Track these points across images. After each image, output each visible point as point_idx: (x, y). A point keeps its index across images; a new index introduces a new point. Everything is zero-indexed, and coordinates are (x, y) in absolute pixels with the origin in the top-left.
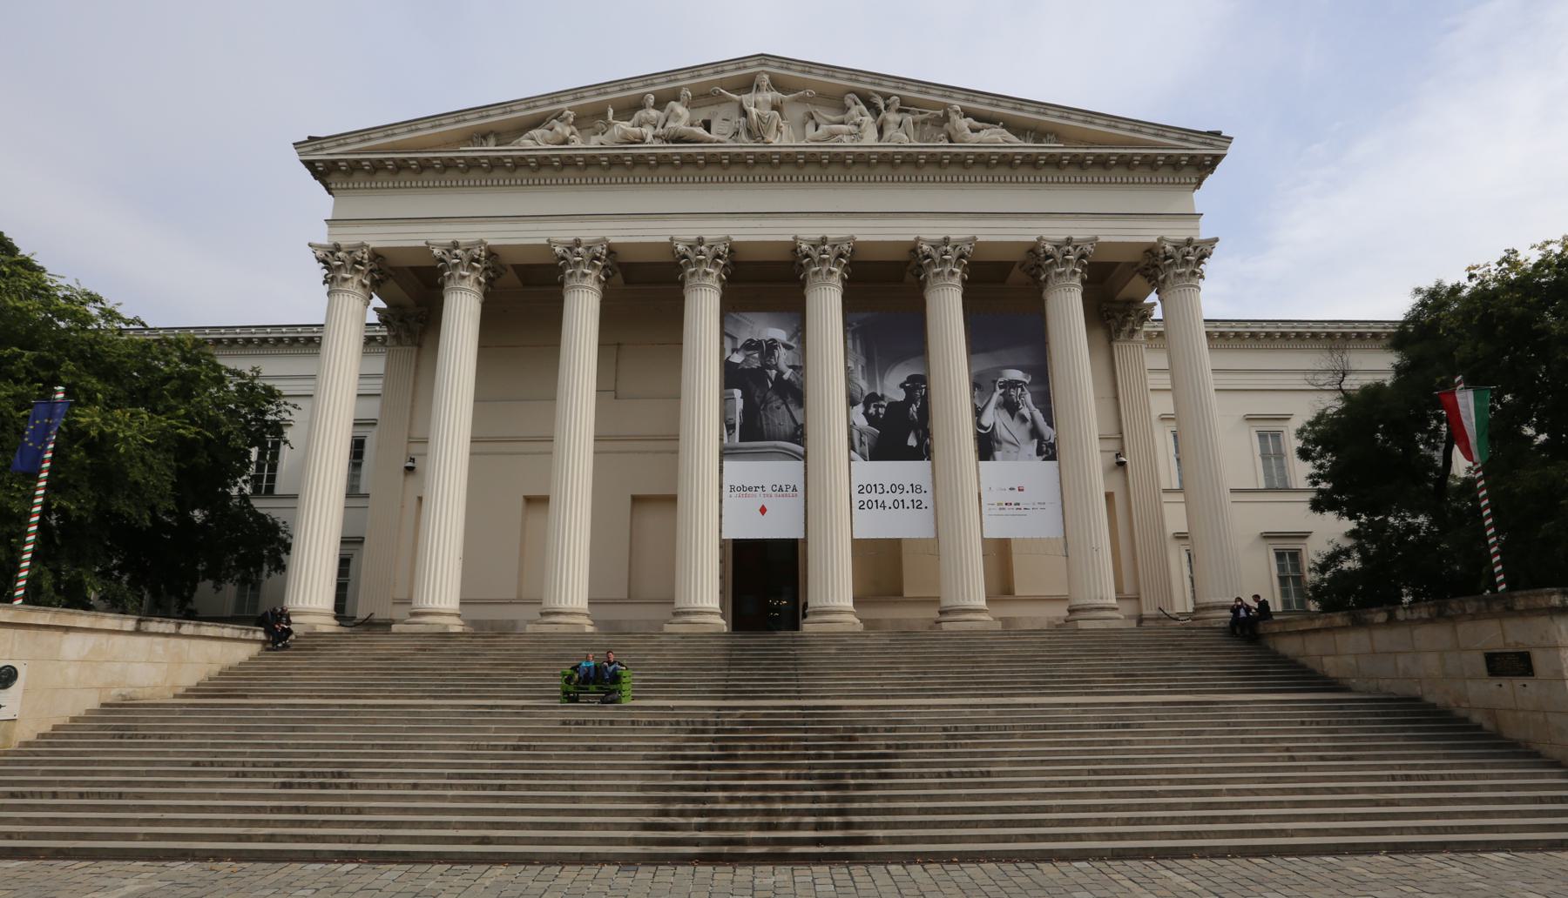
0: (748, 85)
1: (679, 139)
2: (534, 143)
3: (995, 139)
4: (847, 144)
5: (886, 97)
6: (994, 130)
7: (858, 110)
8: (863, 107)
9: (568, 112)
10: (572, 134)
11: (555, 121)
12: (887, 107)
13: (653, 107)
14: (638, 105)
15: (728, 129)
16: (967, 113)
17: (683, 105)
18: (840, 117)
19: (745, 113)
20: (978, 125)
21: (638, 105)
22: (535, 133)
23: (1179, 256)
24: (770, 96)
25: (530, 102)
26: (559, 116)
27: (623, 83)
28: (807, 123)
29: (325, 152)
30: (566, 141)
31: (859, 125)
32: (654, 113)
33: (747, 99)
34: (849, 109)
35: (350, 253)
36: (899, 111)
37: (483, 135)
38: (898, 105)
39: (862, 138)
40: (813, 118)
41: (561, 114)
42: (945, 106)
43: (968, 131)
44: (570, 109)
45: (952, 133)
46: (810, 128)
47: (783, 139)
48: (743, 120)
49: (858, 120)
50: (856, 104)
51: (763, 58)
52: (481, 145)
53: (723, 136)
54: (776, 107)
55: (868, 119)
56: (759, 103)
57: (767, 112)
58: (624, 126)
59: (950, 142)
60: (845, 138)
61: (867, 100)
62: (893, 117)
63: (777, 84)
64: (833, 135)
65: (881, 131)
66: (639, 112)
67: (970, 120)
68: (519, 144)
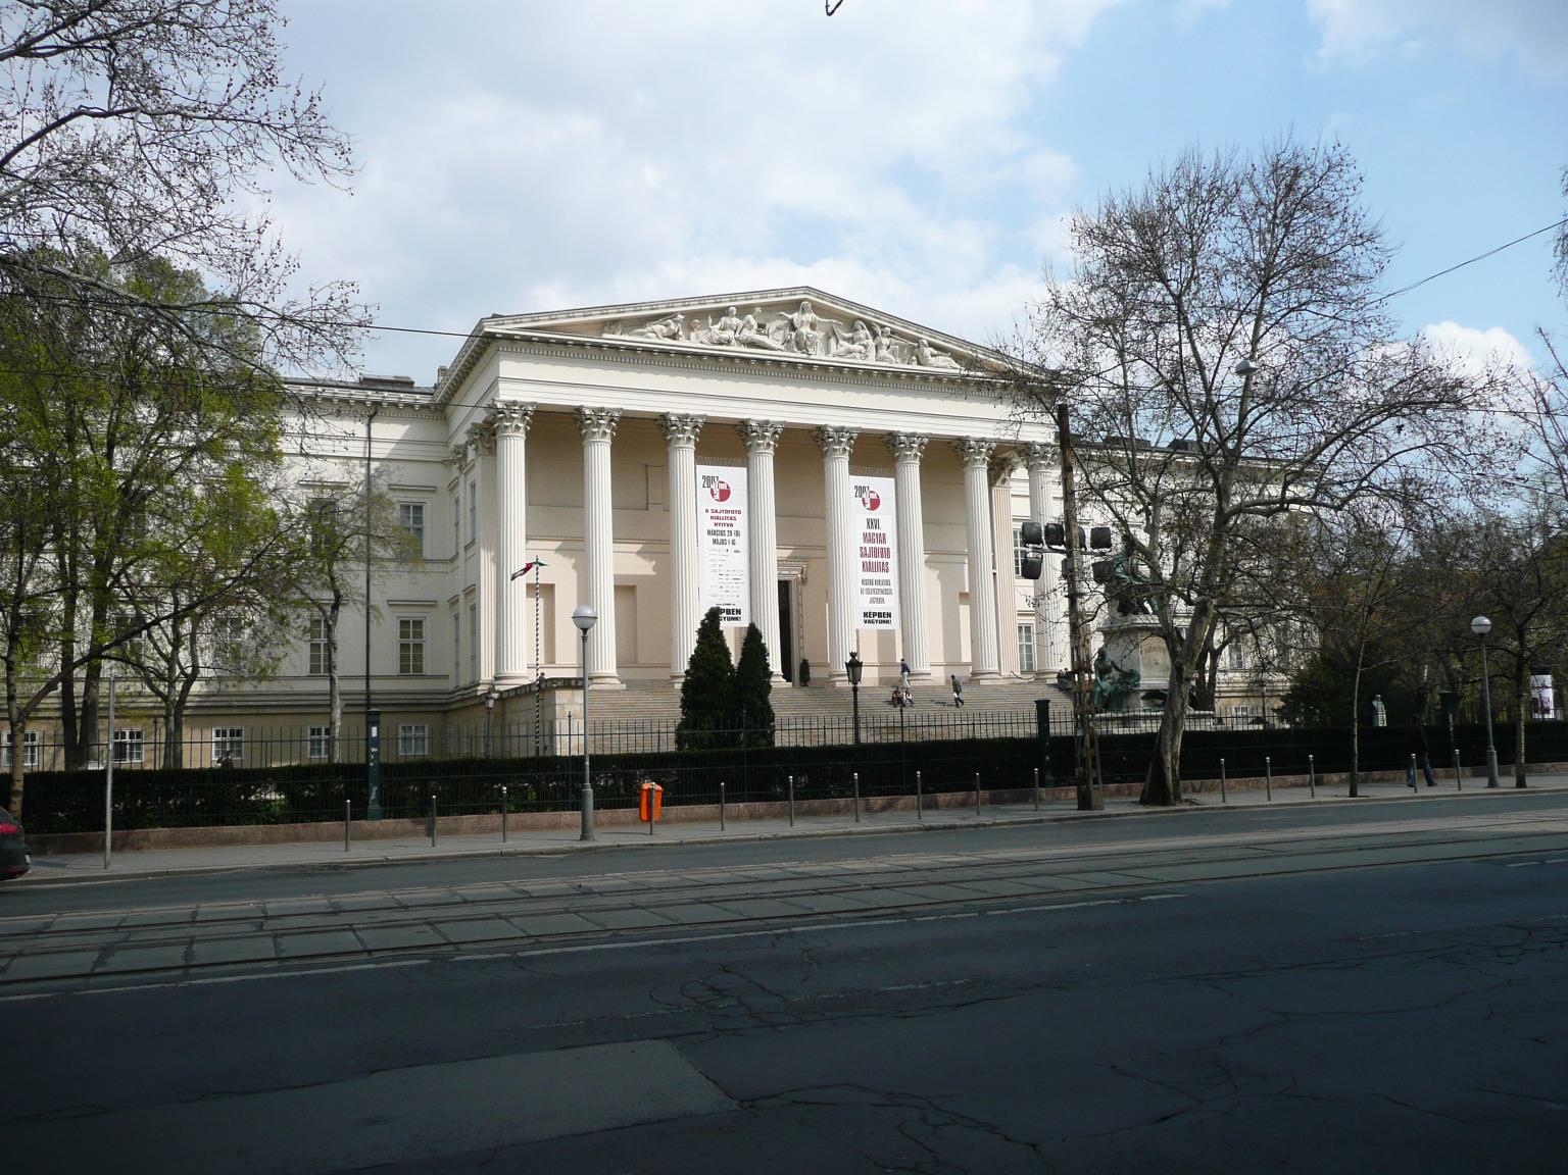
0: (796, 305)
1: (753, 344)
2: (653, 337)
3: (944, 365)
4: (857, 361)
5: (883, 327)
7: (864, 333)
8: (868, 332)
9: (680, 317)
11: (670, 321)
12: (882, 332)
13: (736, 316)
14: (723, 312)
15: (780, 335)
16: (931, 345)
18: (851, 335)
19: (793, 328)
20: (935, 352)
21: (723, 312)
22: (658, 327)
23: (1042, 452)
24: (810, 316)
25: (653, 305)
26: (671, 315)
27: (716, 298)
28: (829, 338)
29: (505, 327)
30: (674, 336)
31: (866, 347)
32: (735, 321)
33: (795, 316)
34: (857, 330)
35: (522, 406)
36: (890, 336)
37: (612, 325)
39: (867, 356)
40: (834, 334)
41: (675, 317)
42: (916, 340)
43: (930, 358)
44: (682, 313)
45: (920, 357)
46: (833, 341)
48: (794, 334)
49: (865, 342)
50: (863, 328)
51: (808, 289)
53: (776, 345)
54: (813, 326)
55: (870, 341)
59: (919, 364)
60: (858, 355)
61: (870, 326)
62: (886, 341)
63: (817, 309)
64: (850, 352)
65: (876, 347)
66: (723, 319)
67: (931, 349)
68: (642, 334)
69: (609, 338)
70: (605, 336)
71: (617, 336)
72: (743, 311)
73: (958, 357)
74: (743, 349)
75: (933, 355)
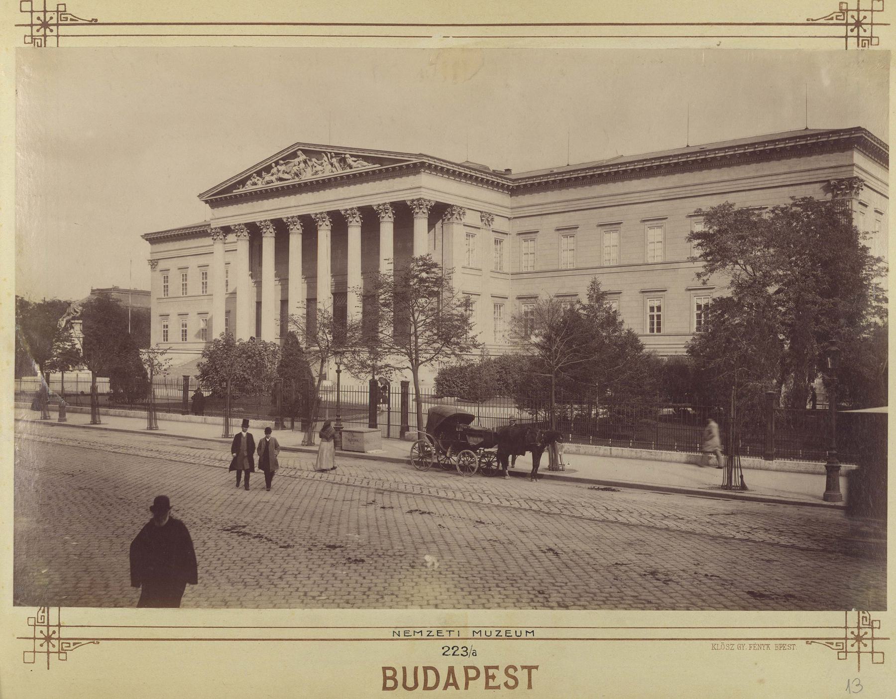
0: (294, 155)
1: (281, 179)
2: (249, 187)
5: (330, 153)
6: (359, 162)
8: (326, 158)
10: (258, 180)
16: (352, 156)
17: (280, 165)
20: (355, 159)
24: (303, 157)
33: (297, 160)
38: (334, 156)
44: (255, 173)
47: (308, 176)
52: (239, 189)
54: (305, 162)
56: (296, 164)
57: (302, 165)
58: (268, 177)
62: (334, 160)
69: (236, 192)
70: (234, 191)
71: (241, 190)
72: (277, 163)
73: (366, 159)
74: (279, 183)
75: (355, 161)
